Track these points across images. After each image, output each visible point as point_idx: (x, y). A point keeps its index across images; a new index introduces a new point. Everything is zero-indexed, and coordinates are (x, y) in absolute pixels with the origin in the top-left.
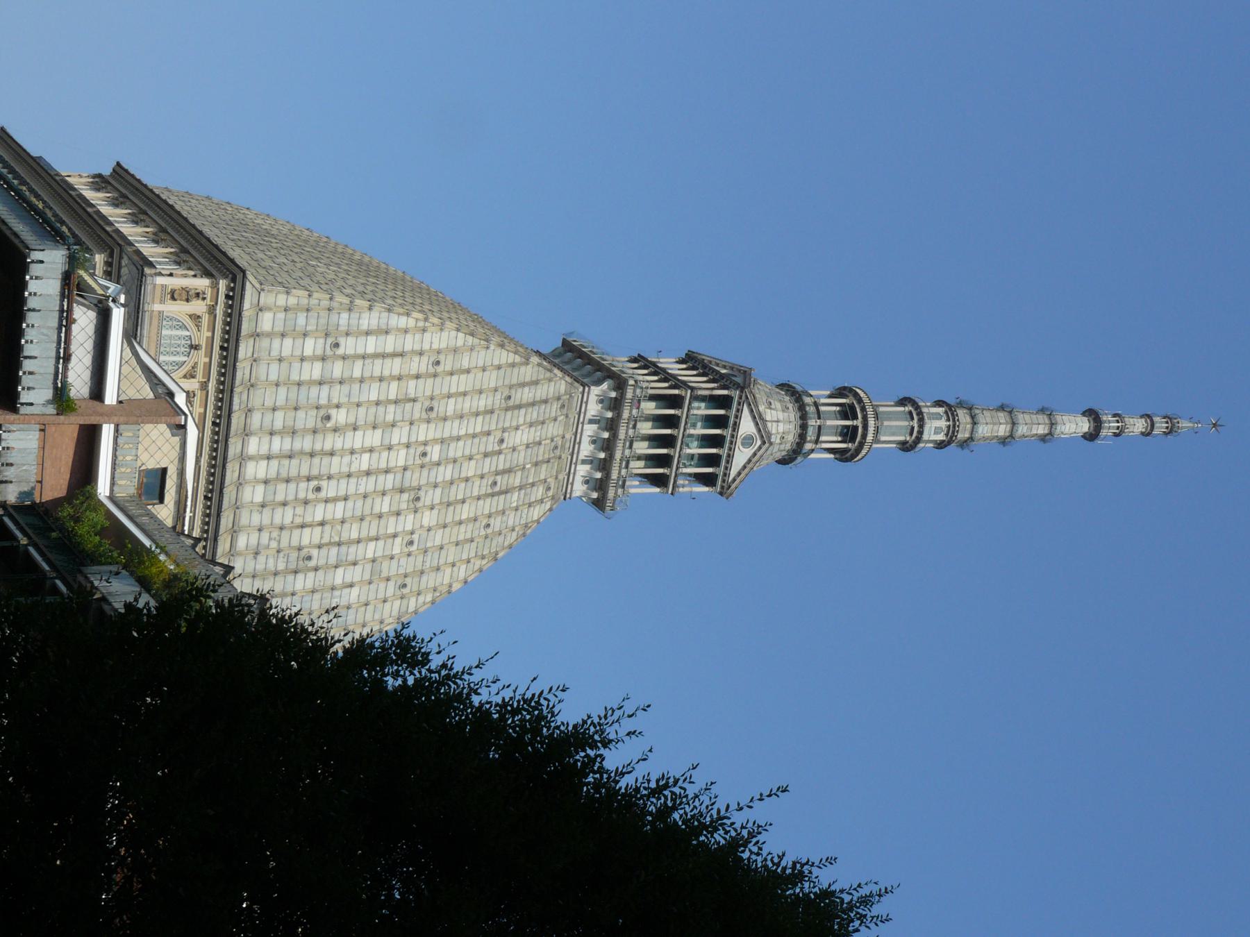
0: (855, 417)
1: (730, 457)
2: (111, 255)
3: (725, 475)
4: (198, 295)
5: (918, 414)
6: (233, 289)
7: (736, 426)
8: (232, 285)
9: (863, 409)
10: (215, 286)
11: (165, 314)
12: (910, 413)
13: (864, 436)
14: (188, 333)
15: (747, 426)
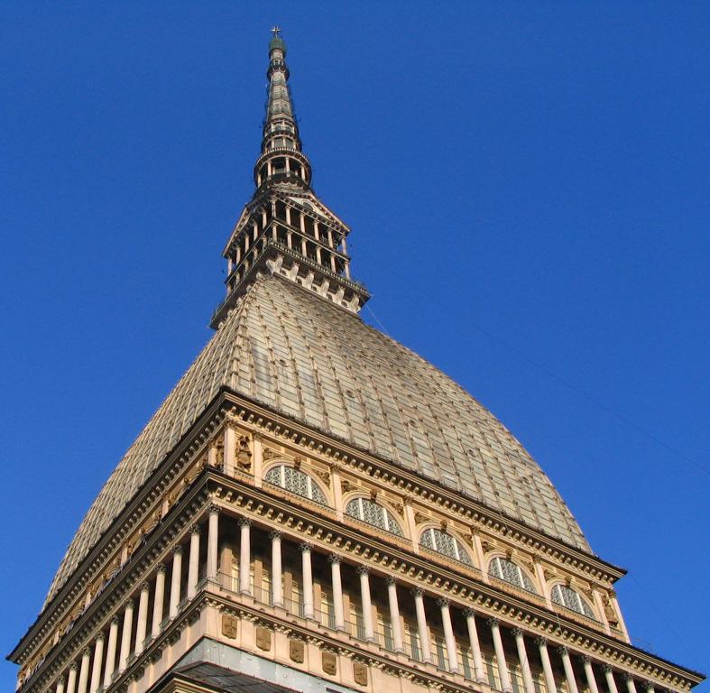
0: (283, 159)
1: (320, 218)
2: (212, 486)
3: (333, 226)
4: (243, 443)
5: (278, 134)
6: (239, 409)
7: (297, 205)
8: (234, 408)
9: (277, 153)
10: (236, 425)
11: (264, 478)
12: (276, 138)
13: (297, 156)
14: (283, 468)
15: (300, 201)
